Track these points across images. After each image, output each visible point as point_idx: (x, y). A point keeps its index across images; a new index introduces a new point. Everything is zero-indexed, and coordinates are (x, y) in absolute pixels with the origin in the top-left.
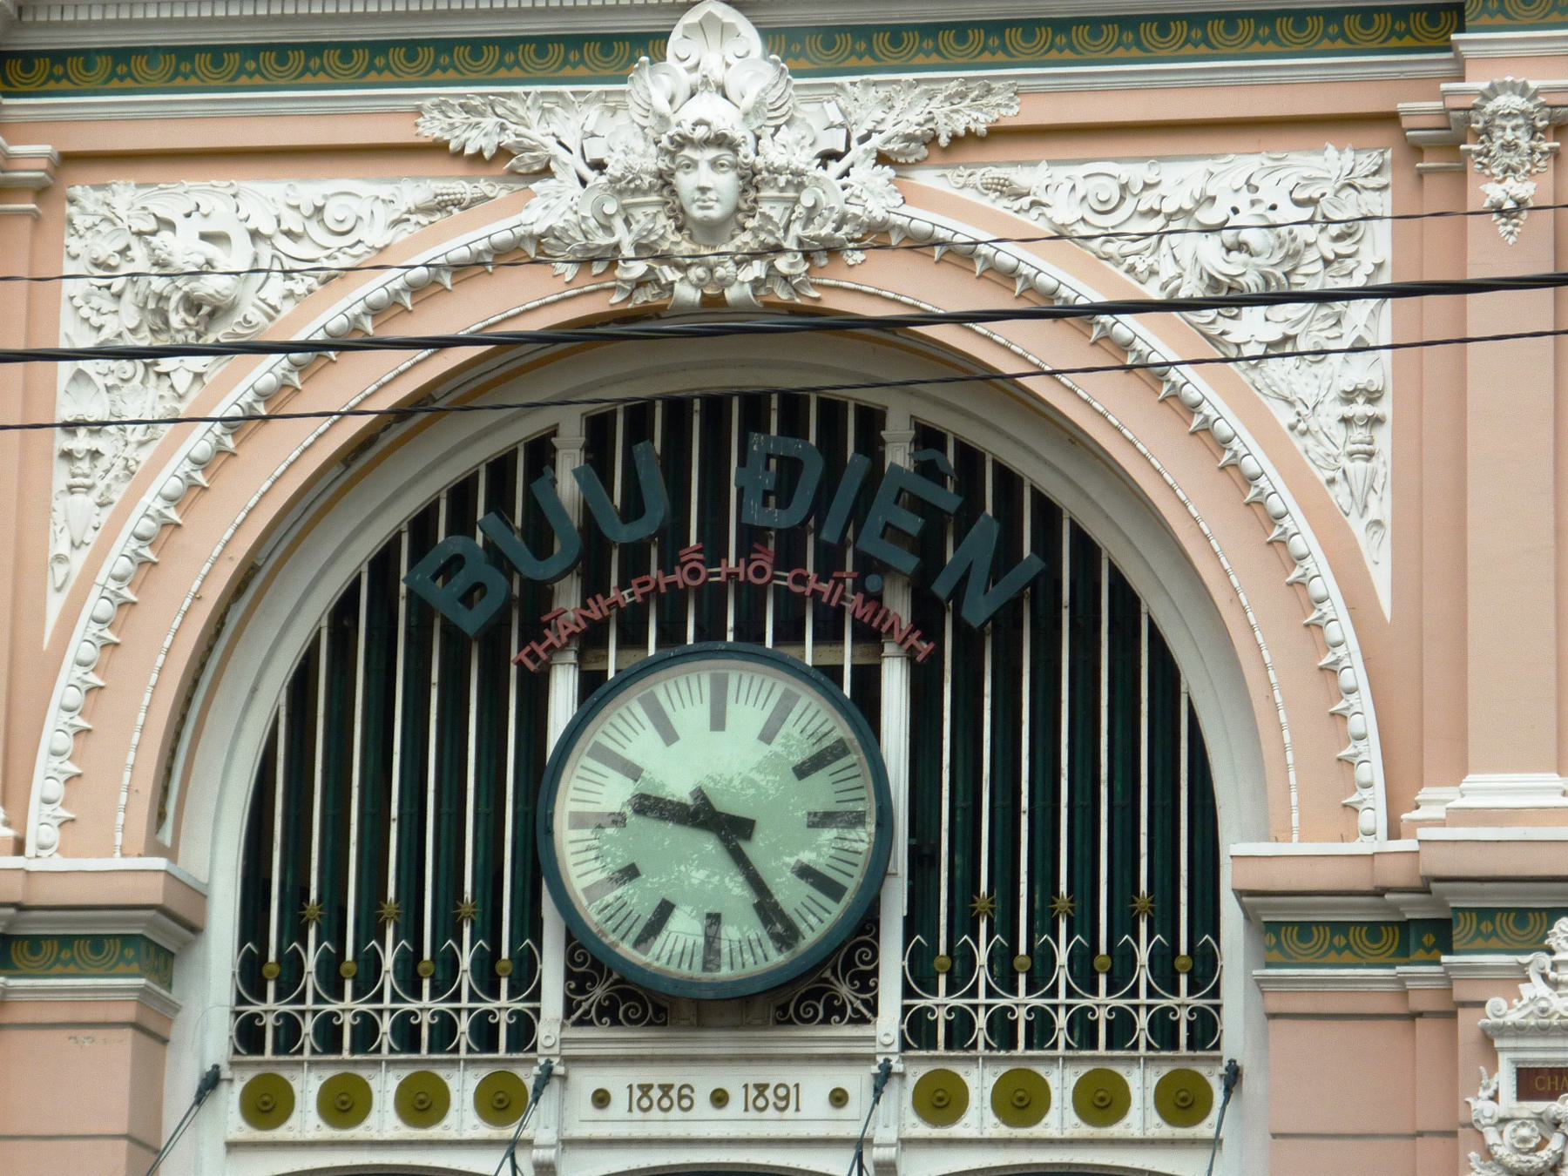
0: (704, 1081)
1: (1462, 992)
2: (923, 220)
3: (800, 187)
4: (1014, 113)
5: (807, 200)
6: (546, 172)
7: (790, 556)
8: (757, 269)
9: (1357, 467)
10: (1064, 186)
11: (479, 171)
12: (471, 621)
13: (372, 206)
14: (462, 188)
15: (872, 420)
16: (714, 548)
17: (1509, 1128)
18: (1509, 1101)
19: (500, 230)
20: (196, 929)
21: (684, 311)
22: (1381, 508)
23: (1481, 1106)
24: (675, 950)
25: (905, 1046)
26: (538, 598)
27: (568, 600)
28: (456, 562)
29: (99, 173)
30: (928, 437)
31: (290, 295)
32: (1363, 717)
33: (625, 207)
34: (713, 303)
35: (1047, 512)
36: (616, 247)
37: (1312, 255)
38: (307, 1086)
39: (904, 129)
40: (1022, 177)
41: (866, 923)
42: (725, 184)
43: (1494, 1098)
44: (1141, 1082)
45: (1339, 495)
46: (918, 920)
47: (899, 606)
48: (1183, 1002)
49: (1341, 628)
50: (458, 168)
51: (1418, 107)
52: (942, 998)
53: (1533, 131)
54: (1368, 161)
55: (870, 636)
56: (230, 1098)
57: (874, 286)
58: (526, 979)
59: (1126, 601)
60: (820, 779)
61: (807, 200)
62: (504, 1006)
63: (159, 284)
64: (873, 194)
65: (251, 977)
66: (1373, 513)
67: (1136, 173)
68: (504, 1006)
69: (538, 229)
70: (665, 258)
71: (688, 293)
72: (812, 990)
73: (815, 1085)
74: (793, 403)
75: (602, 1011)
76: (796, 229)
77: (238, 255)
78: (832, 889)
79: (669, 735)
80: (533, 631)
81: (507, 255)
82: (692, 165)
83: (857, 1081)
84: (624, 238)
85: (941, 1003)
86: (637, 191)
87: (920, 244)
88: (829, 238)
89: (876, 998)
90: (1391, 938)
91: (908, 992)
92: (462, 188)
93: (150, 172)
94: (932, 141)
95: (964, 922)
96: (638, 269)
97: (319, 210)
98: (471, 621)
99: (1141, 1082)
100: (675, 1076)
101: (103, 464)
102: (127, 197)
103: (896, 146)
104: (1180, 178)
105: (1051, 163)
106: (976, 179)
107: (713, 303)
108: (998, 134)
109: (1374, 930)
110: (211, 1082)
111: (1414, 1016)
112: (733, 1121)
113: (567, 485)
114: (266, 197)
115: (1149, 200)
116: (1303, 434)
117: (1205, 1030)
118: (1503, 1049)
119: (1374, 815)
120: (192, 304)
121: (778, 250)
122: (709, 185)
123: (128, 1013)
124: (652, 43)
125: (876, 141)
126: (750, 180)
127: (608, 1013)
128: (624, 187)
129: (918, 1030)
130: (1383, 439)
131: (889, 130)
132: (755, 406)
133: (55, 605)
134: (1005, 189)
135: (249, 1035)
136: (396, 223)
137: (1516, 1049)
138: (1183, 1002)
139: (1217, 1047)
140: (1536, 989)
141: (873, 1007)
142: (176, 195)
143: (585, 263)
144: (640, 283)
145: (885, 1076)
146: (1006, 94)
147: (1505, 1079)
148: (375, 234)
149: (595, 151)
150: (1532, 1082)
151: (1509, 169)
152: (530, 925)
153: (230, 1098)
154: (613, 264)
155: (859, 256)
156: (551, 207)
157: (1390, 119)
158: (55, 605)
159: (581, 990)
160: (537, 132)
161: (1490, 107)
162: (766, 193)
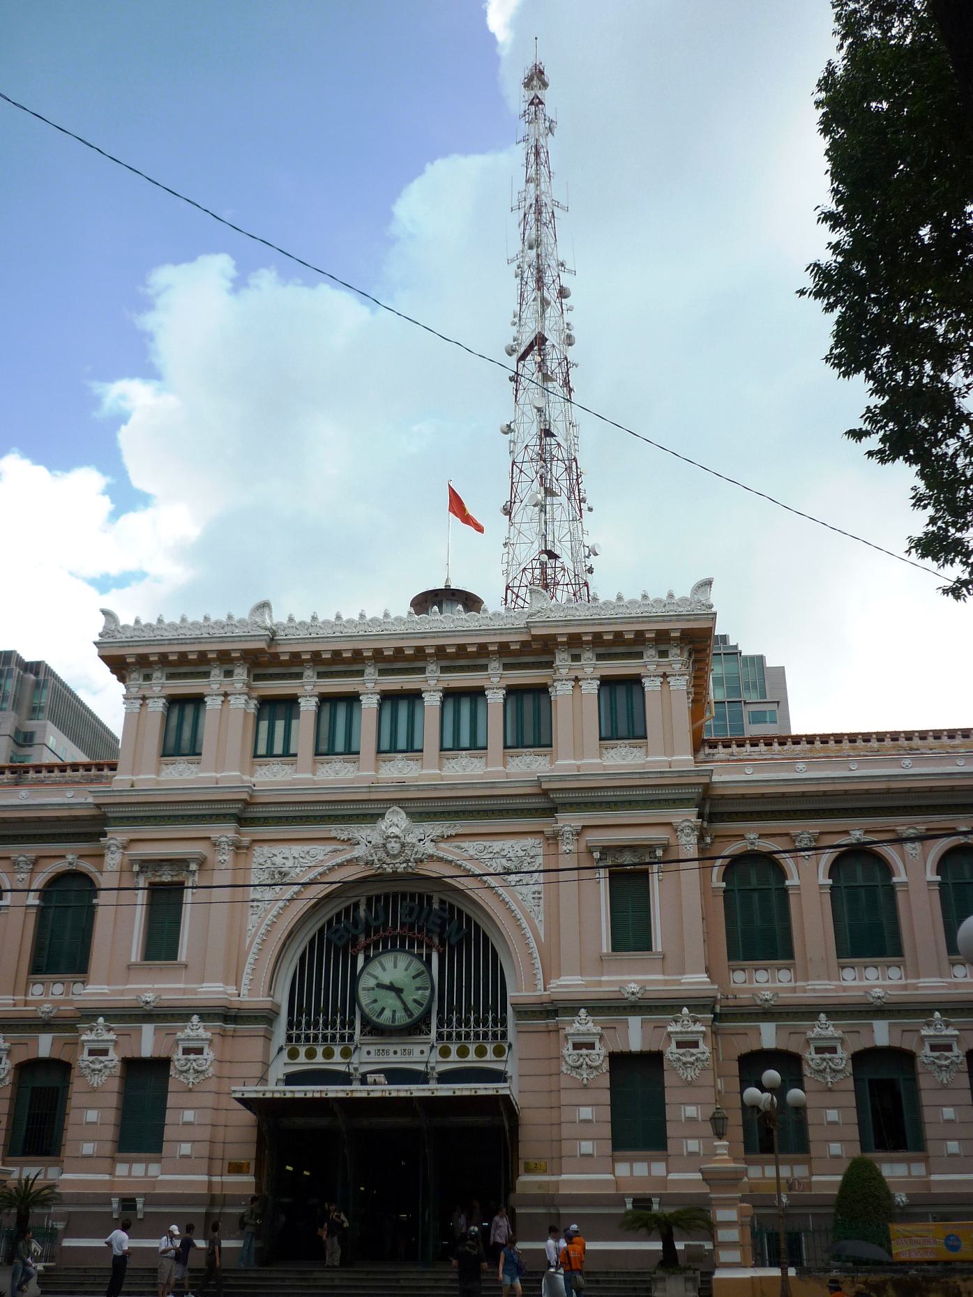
0: (392, 1048)
2: (441, 854)
4: (460, 831)
7: (411, 928)
10: (472, 847)
13: (320, 852)
14: (340, 847)
15: (430, 899)
19: (348, 857)
21: (389, 874)
22: (541, 917)
23: (565, 1052)
24: (385, 1018)
26: (355, 938)
27: (362, 939)
28: (337, 930)
30: (442, 902)
32: (538, 964)
35: (469, 919)
38: (302, 1050)
40: (463, 845)
41: (428, 1013)
42: (398, 846)
44: (490, 1048)
45: (532, 914)
46: (440, 1011)
47: (436, 941)
49: (533, 944)
51: (548, 830)
54: (537, 841)
55: (429, 947)
56: (285, 1053)
58: (352, 1026)
59: (486, 939)
64: (430, 848)
65: (290, 1025)
67: (487, 844)
72: (416, 1027)
74: (412, 896)
77: (290, 863)
78: (421, 1005)
79: (384, 969)
80: (354, 946)
81: (349, 862)
83: (426, 1048)
84: (375, 858)
85: (445, 1030)
87: (441, 859)
92: (340, 847)
95: (450, 1012)
98: (340, 944)
99: (490, 1048)
100: (385, 1047)
102: (266, 850)
104: (497, 845)
108: (457, 835)
109: (541, 1012)
110: (281, 1049)
113: (362, 913)
114: (296, 849)
117: (504, 1035)
119: (541, 986)
120: (280, 873)
122: (394, 846)
124: (382, 816)
126: (403, 845)
127: (370, 1033)
128: (375, 847)
129: (440, 1036)
130: (542, 902)
132: (404, 895)
134: (458, 847)
135: (289, 1038)
138: (499, 1029)
145: (433, 1047)
147: (570, 1046)
148: (321, 858)
150: (577, 1046)
152: (353, 1013)
153: (285, 1053)
156: (359, 852)
157: (542, 832)
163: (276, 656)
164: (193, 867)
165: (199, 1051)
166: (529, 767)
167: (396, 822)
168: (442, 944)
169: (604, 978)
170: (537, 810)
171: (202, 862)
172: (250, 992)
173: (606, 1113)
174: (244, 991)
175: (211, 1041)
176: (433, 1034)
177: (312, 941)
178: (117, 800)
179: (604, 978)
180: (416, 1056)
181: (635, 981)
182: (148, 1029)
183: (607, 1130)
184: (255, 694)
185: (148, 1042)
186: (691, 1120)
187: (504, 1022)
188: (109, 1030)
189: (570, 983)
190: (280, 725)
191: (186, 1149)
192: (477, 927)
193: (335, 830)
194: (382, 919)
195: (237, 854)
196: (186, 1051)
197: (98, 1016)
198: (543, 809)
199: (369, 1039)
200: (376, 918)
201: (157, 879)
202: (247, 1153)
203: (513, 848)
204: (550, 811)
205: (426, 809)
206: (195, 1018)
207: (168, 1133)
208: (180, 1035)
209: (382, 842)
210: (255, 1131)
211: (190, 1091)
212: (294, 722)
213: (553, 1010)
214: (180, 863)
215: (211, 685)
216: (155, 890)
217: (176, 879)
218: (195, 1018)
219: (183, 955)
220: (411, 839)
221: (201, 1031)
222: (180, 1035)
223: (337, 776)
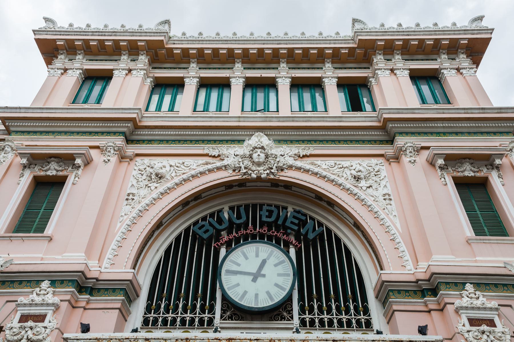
1: (447, 300)
3: (276, 158)
5: (278, 160)
8: (268, 171)
9: (389, 206)
11: (215, 159)
12: (205, 236)
16: (255, 228)
17: (471, 333)
18: (468, 327)
20: (138, 296)
25: (300, 326)
26: (218, 236)
28: (203, 226)
31: (176, 176)
33: (242, 161)
36: (241, 167)
37: (372, 173)
39: (294, 153)
42: (263, 156)
43: (464, 325)
46: (301, 298)
47: (292, 239)
48: (362, 317)
52: (307, 316)
53: (414, 150)
55: (287, 245)
58: (212, 309)
59: (338, 240)
60: (280, 267)
61: (278, 160)
62: (206, 316)
63: (151, 170)
65: (148, 309)
66: (394, 214)
68: (206, 316)
69: (226, 164)
70: (250, 169)
71: (254, 176)
75: (229, 318)
76: (276, 165)
80: (217, 240)
81: (219, 169)
86: (245, 157)
87: (299, 169)
88: (281, 167)
89: (292, 316)
90: (419, 294)
91: (299, 314)
92: (210, 160)
94: (299, 156)
95: (310, 299)
96: (245, 171)
97: (183, 163)
98: (205, 236)
101: (134, 201)
102: (146, 160)
103: (293, 156)
104: (346, 162)
105: (321, 161)
106: (308, 162)
111: (429, 312)
113: (226, 216)
115: (340, 166)
116: (377, 201)
118: (463, 313)
120: (157, 175)
121: (272, 168)
123: (118, 305)
125: (289, 154)
127: (230, 318)
129: (303, 323)
130: (392, 202)
131: (291, 153)
133: (119, 225)
134: (312, 164)
136: (198, 166)
137: (466, 313)
139: (372, 328)
140: (465, 299)
141: (292, 318)
143: (234, 171)
144: (245, 174)
146: (312, 149)
148: (194, 167)
149: (236, 153)
151: (411, 156)
152: (213, 298)
154: (240, 171)
155: (287, 171)
156: (229, 161)
159: (224, 313)
161: (406, 146)
162: (270, 158)
163: (170, 50)
164: (78, 161)
165: (41, 318)
168: (298, 239)
169: (477, 258)
171: (88, 162)
172: (113, 264)
174: (106, 263)
175: (57, 307)
176: (296, 321)
177: (178, 239)
179: (477, 258)
184: (151, 75)
187: (366, 311)
190: (167, 99)
192: (329, 231)
194: (244, 218)
195: (120, 162)
200: (239, 217)
208: (22, 299)
209: (248, 153)
212: (179, 97)
213: (430, 288)
214: (67, 159)
215: (120, 66)
217: (61, 173)
218: (45, 284)
219: (49, 230)
221: (50, 295)
222: (22, 299)
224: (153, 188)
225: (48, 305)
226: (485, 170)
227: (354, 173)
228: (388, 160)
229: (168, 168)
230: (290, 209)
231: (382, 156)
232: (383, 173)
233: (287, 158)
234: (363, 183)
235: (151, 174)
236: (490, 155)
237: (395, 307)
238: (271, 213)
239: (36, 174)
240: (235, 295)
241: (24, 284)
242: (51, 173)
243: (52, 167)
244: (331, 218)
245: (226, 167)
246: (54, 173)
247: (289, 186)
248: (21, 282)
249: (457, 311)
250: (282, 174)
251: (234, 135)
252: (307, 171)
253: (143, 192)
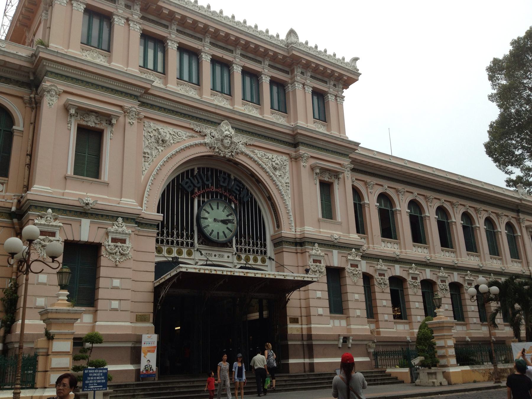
0: (214, 253)
1: (307, 250)
6: (206, 135)
10: (259, 153)
13: (183, 133)
15: (229, 175)
18: (312, 263)
19: (202, 141)
24: (214, 237)
27: (196, 190)
29: (148, 120)
32: (292, 219)
34: (224, 157)
40: (256, 151)
50: (193, 132)
55: (230, 201)
57: (241, 159)
58: (192, 237)
73: (226, 255)
81: (201, 144)
82: (227, 139)
83: (230, 255)
87: (246, 155)
92: (195, 135)
93: (155, 122)
99: (259, 258)
107: (224, 157)
111: (297, 253)
112: (216, 259)
117: (265, 253)
119: (294, 230)
124: (219, 124)
127: (202, 243)
128: (217, 139)
133: (143, 177)
142: (159, 126)
143: (210, 148)
152: (192, 231)
156: (207, 140)
158: (143, 177)
160: (204, 130)
165: (123, 241)
166: (278, 120)
167: (227, 129)
170: (287, 142)
173: (326, 295)
176: (235, 249)
177: (168, 186)
178: (60, 60)
179: (321, 230)
180: (225, 259)
181: (336, 234)
182: (86, 222)
183: (326, 303)
185: (86, 231)
186: (357, 300)
187: (265, 246)
188: (56, 219)
189: (310, 230)
190: (151, 53)
191: (115, 304)
193: (193, 124)
196: (114, 240)
197: (48, 208)
198: (289, 143)
199: (202, 247)
201: (84, 123)
202: (149, 308)
203: (278, 159)
204: (295, 145)
205: (245, 127)
206: (120, 220)
207: (102, 293)
210: (152, 294)
211: (116, 266)
213: (301, 243)
216: (82, 130)
220: (235, 140)
223: (188, 92)
224: (160, 150)
225: (126, 234)
226: (333, 178)
227: (274, 164)
228: (291, 158)
229: (168, 135)
230: (232, 177)
231: (288, 154)
232: (288, 168)
233: (241, 145)
234: (277, 173)
235: (159, 138)
236: (339, 172)
237: (284, 250)
238: (225, 179)
239: (79, 122)
240: (207, 231)
241: (104, 217)
242: (91, 124)
243: (92, 120)
244: (254, 188)
245: (205, 144)
246: (93, 125)
247: (237, 164)
248: (102, 216)
249: (310, 256)
250: (237, 157)
251: (212, 119)
252: (251, 158)
253: (154, 153)
